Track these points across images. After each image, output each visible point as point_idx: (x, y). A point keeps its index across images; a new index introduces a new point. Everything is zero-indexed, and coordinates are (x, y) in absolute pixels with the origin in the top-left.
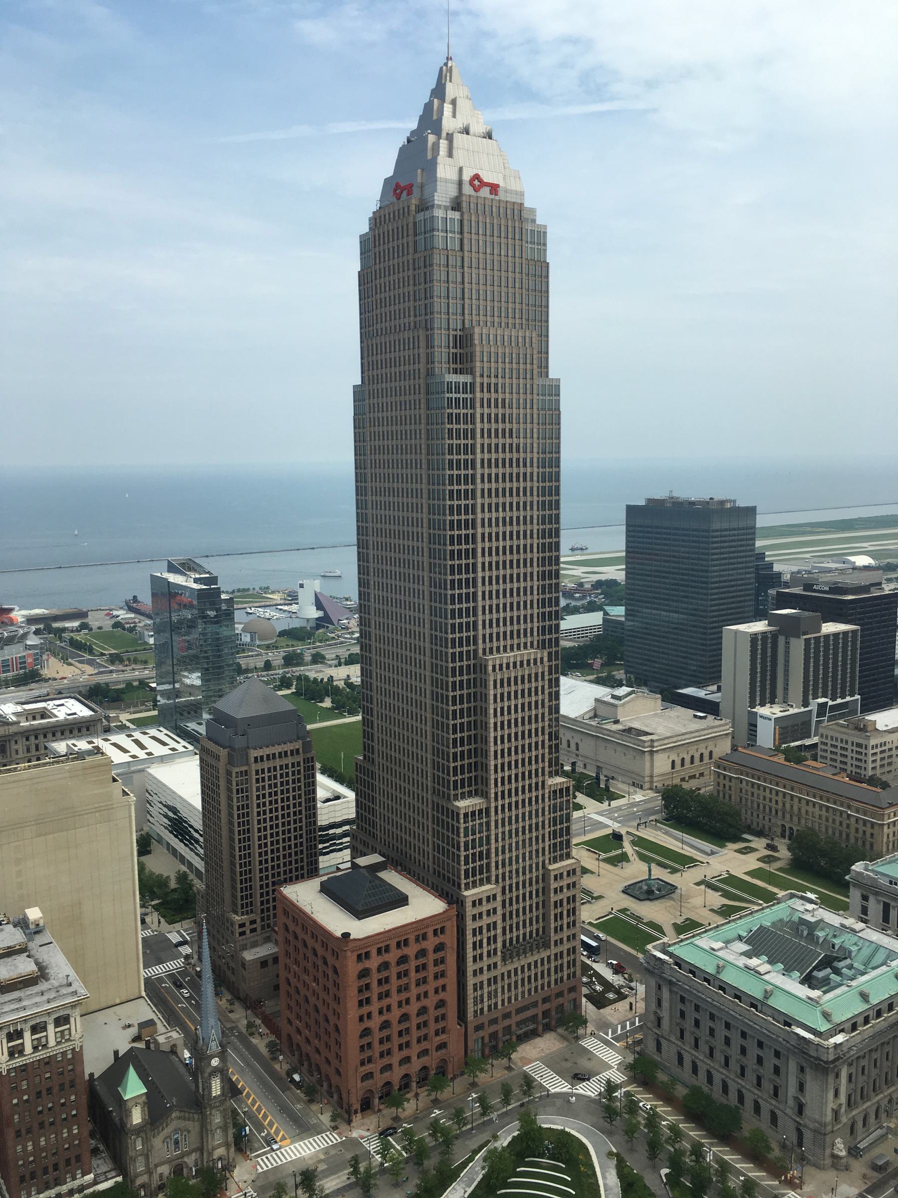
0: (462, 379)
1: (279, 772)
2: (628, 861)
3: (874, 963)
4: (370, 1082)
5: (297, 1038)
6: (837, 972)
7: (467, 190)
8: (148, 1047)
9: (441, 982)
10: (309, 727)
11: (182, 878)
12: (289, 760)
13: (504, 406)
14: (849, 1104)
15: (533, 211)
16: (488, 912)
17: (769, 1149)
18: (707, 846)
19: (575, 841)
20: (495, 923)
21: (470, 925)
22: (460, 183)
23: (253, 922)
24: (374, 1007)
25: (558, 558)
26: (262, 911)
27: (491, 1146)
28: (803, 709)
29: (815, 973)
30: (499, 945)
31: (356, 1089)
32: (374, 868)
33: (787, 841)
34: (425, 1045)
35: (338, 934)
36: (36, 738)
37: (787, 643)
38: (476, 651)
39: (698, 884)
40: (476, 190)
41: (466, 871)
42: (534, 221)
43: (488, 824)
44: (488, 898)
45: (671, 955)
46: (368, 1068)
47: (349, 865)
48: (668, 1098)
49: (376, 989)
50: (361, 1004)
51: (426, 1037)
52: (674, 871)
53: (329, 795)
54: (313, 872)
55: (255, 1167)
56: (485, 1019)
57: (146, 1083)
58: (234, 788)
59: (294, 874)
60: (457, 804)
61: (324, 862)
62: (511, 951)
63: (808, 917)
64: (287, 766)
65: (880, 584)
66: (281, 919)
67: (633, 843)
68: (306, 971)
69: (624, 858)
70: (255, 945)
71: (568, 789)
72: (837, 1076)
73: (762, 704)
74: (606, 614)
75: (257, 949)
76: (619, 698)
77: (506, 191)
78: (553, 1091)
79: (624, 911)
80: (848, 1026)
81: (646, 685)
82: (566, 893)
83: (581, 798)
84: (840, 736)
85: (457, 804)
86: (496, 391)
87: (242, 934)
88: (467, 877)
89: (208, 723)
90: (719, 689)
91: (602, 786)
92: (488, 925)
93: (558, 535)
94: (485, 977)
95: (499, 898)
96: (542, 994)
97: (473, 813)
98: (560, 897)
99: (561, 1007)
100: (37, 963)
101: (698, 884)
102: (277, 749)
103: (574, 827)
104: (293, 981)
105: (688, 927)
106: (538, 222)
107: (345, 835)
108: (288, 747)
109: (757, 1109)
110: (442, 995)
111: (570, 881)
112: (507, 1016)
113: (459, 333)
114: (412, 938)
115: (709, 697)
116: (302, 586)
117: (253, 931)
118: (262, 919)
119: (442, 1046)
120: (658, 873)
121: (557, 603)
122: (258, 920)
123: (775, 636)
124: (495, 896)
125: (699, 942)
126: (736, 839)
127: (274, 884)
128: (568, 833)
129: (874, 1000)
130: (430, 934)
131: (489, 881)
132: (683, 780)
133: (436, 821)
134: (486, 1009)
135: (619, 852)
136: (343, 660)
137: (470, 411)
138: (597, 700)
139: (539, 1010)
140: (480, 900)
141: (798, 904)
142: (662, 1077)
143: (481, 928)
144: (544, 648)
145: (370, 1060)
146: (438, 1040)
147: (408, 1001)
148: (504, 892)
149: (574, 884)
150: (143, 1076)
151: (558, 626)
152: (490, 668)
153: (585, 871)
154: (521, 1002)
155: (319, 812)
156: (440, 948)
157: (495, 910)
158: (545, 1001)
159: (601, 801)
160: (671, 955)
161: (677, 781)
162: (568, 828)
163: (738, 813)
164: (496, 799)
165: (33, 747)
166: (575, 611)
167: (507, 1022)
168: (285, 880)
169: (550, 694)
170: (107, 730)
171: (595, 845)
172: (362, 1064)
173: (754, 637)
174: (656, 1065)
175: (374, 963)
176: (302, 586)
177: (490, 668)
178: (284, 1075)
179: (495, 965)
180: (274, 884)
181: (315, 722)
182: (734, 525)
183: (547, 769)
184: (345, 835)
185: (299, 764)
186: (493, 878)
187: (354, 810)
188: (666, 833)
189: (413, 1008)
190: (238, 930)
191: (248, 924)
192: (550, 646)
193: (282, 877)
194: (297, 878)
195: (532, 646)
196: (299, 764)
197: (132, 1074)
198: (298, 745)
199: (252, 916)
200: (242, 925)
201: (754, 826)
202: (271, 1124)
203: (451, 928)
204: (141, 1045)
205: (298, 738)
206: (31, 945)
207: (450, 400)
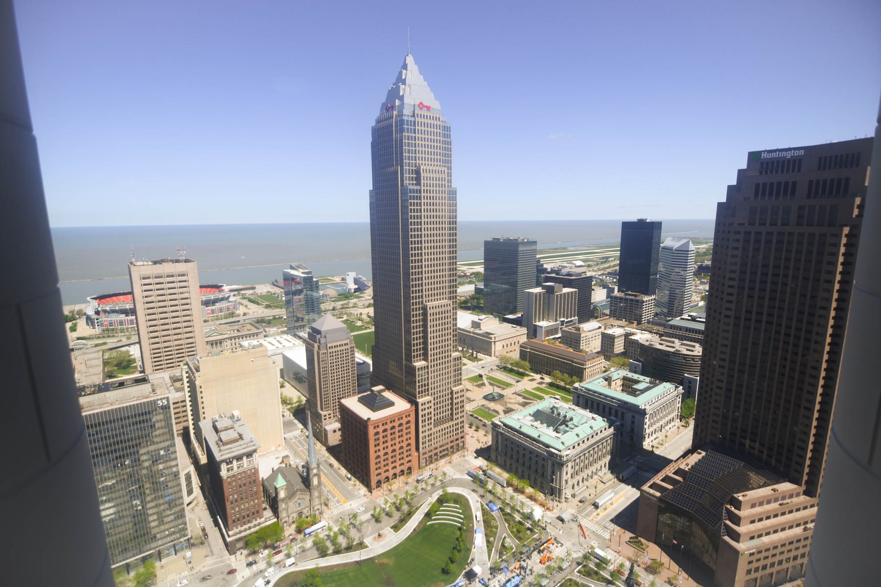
0: (415, 187)
1: (339, 353)
2: (485, 385)
4: (380, 476)
6: (567, 426)
7: (417, 108)
8: (286, 466)
11: (299, 398)
12: (344, 348)
13: (433, 199)
14: (572, 477)
19: (463, 379)
20: (431, 412)
21: (420, 413)
22: (414, 105)
23: (330, 414)
24: (381, 447)
25: (456, 262)
26: (333, 410)
28: (555, 323)
30: (433, 421)
31: (374, 480)
32: (380, 391)
34: (402, 461)
36: (235, 339)
37: (549, 297)
38: (422, 302)
39: (513, 394)
40: (421, 109)
41: (419, 392)
43: (428, 372)
46: (379, 471)
49: (382, 440)
50: (375, 446)
51: (402, 458)
52: (503, 389)
55: (332, 512)
56: (427, 449)
57: (286, 480)
59: (347, 395)
60: (415, 364)
62: (437, 423)
65: (585, 272)
67: (487, 379)
69: (483, 384)
70: (331, 423)
71: (461, 357)
72: (567, 466)
73: (539, 321)
74: (476, 285)
75: (331, 425)
76: (481, 320)
77: (433, 109)
78: (454, 477)
79: (483, 406)
80: (572, 447)
81: (492, 315)
82: (460, 399)
83: (465, 361)
86: (430, 193)
88: (419, 393)
89: (309, 333)
91: (475, 356)
94: (427, 434)
95: (433, 402)
96: (450, 439)
97: (422, 368)
99: (458, 444)
100: (238, 433)
101: (513, 394)
102: (338, 343)
105: (508, 411)
108: (343, 342)
110: (409, 441)
111: (462, 394)
112: (436, 448)
113: (414, 168)
114: (396, 419)
116: (348, 275)
117: (330, 418)
118: (334, 413)
119: (410, 461)
121: (456, 281)
122: (332, 414)
124: (431, 402)
127: (338, 399)
129: (581, 436)
130: (404, 416)
131: (428, 395)
132: (507, 352)
134: (427, 446)
135: (482, 382)
137: (419, 201)
141: (553, 401)
143: (425, 414)
144: (450, 299)
145: (379, 468)
146: (407, 459)
147: (395, 444)
148: (434, 400)
149: (463, 396)
150: (285, 477)
151: (456, 291)
152: (428, 308)
153: (467, 390)
154: (441, 443)
156: (408, 422)
157: (431, 407)
158: (452, 442)
161: (505, 353)
162: (461, 373)
164: (431, 362)
165: (234, 344)
168: (343, 397)
169: (453, 319)
170: (265, 336)
171: (472, 380)
172: (376, 469)
175: (381, 429)
176: (348, 275)
179: (431, 429)
182: (528, 248)
183: (452, 349)
185: (348, 349)
186: (430, 394)
189: (397, 447)
192: (453, 299)
195: (446, 299)
196: (348, 349)
197: (280, 477)
198: (347, 341)
199: (329, 412)
200: (325, 416)
202: (339, 495)
203: (413, 414)
204: (283, 465)
205: (348, 338)
206: (235, 426)
207: (410, 196)
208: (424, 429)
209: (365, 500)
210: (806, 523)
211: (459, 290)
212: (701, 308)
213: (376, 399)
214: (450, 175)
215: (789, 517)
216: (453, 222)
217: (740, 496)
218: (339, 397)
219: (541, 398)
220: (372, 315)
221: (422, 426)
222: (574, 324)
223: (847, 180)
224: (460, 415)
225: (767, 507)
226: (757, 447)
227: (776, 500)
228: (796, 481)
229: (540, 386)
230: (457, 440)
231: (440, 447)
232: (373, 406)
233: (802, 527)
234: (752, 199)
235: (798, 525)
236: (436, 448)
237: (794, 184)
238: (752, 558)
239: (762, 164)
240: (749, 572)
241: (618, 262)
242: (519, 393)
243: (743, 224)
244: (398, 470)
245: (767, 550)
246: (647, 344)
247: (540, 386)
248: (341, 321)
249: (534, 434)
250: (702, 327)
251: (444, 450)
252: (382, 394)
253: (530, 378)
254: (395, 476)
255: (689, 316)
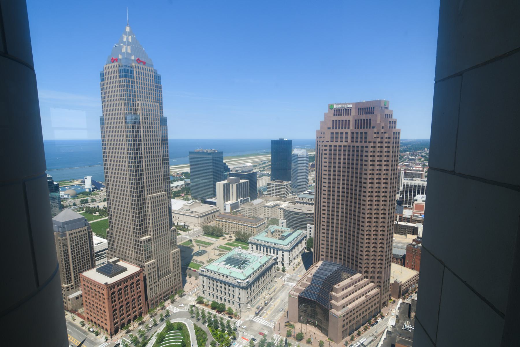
3: (254, 260)
5: (90, 318)
6: (246, 264)
9: (139, 290)
10: (89, 222)
12: (82, 233)
15: (156, 70)
16: (153, 268)
17: (232, 311)
18: (214, 239)
23: (73, 286)
24: (117, 302)
26: (75, 282)
27: (157, 332)
29: (242, 266)
30: (157, 276)
32: (115, 262)
33: (234, 235)
35: (103, 283)
39: (213, 249)
41: (145, 258)
42: (157, 73)
44: (153, 264)
45: (206, 269)
47: (107, 262)
48: (207, 305)
52: (206, 247)
53: (99, 242)
54: (93, 266)
58: (61, 244)
59: (87, 268)
61: (97, 263)
63: (240, 252)
64: (82, 235)
66: (83, 283)
67: (195, 242)
68: (93, 297)
71: (175, 230)
73: (227, 201)
76: (190, 203)
78: (175, 312)
83: (180, 232)
84: (245, 207)
85: (141, 239)
87: (68, 290)
90: (216, 199)
92: (153, 271)
93: (168, 160)
95: (156, 263)
97: (147, 241)
98: (174, 259)
101: (213, 249)
102: (77, 230)
103: (178, 240)
104: (88, 301)
105: (210, 261)
106: (158, 73)
107: (105, 253)
108: (82, 229)
109: (229, 301)
112: (161, 295)
115: (214, 201)
117: (72, 289)
119: (141, 308)
120: (202, 248)
123: (229, 184)
125: (212, 264)
126: (222, 236)
127: (79, 273)
128: (176, 242)
129: (255, 269)
131: (152, 259)
133: (135, 245)
136: (102, 200)
138: (184, 205)
139: (170, 291)
140: (150, 265)
142: (205, 300)
144: (166, 191)
148: (157, 262)
151: (170, 185)
155: (95, 248)
158: (172, 288)
159: (186, 232)
160: (206, 269)
161: (206, 224)
163: (222, 230)
166: (175, 181)
167: (160, 297)
168: (84, 271)
173: (224, 185)
174: (203, 298)
177: (149, 199)
178: (87, 330)
179: (156, 282)
180: (79, 273)
181: (93, 220)
184: (105, 253)
187: (107, 246)
188: (204, 238)
189: (130, 300)
190: (66, 289)
191: (70, 287)
192: (168, 191)
193: (82, 270)
194: (88, 269)
200: (68, 287)
201: (226, 232)
205: (86, 226)
208: (151, 283)
209: (107, 344)
210: (366, 293)
211: (172, 185)
212: (313, 186)
213: (111, 268)
214: (161, 108)
215: (359, 292)
216: (165, 140)
217: (336, 286)
218: (80, 271)
219: (230, 249)
220: (106, 206)
221: (150, 281)
222: (248, 201)
223: (370, 120)
224: (177, 269)
225: (349, 289)
226: (343, 258)
227: (353, 284)
228: (360, 272)
229: (229, 242)
230: (176, 285)
231: (164, 293)
232: (110, 274)
233: (365, 296)
234: (331, 128)
235: (363, 295)
236: (161, 295)
237: (349, 121)
238: (345, 318)
239: (335, 110)
240: (343, 326)
241: (270, 163)
242: (217, 248)
243: (328, 141)
244: (132, 317)
245: (351, 312)
246: (287, 209)
247: (229, 242)
248: (80, 214)
249: (227, 272)
250: (313, 197)
251: (167, 295)
252: (117, 263)
253: (223, 237)
254: (129, 321)
255: (308, 191)
